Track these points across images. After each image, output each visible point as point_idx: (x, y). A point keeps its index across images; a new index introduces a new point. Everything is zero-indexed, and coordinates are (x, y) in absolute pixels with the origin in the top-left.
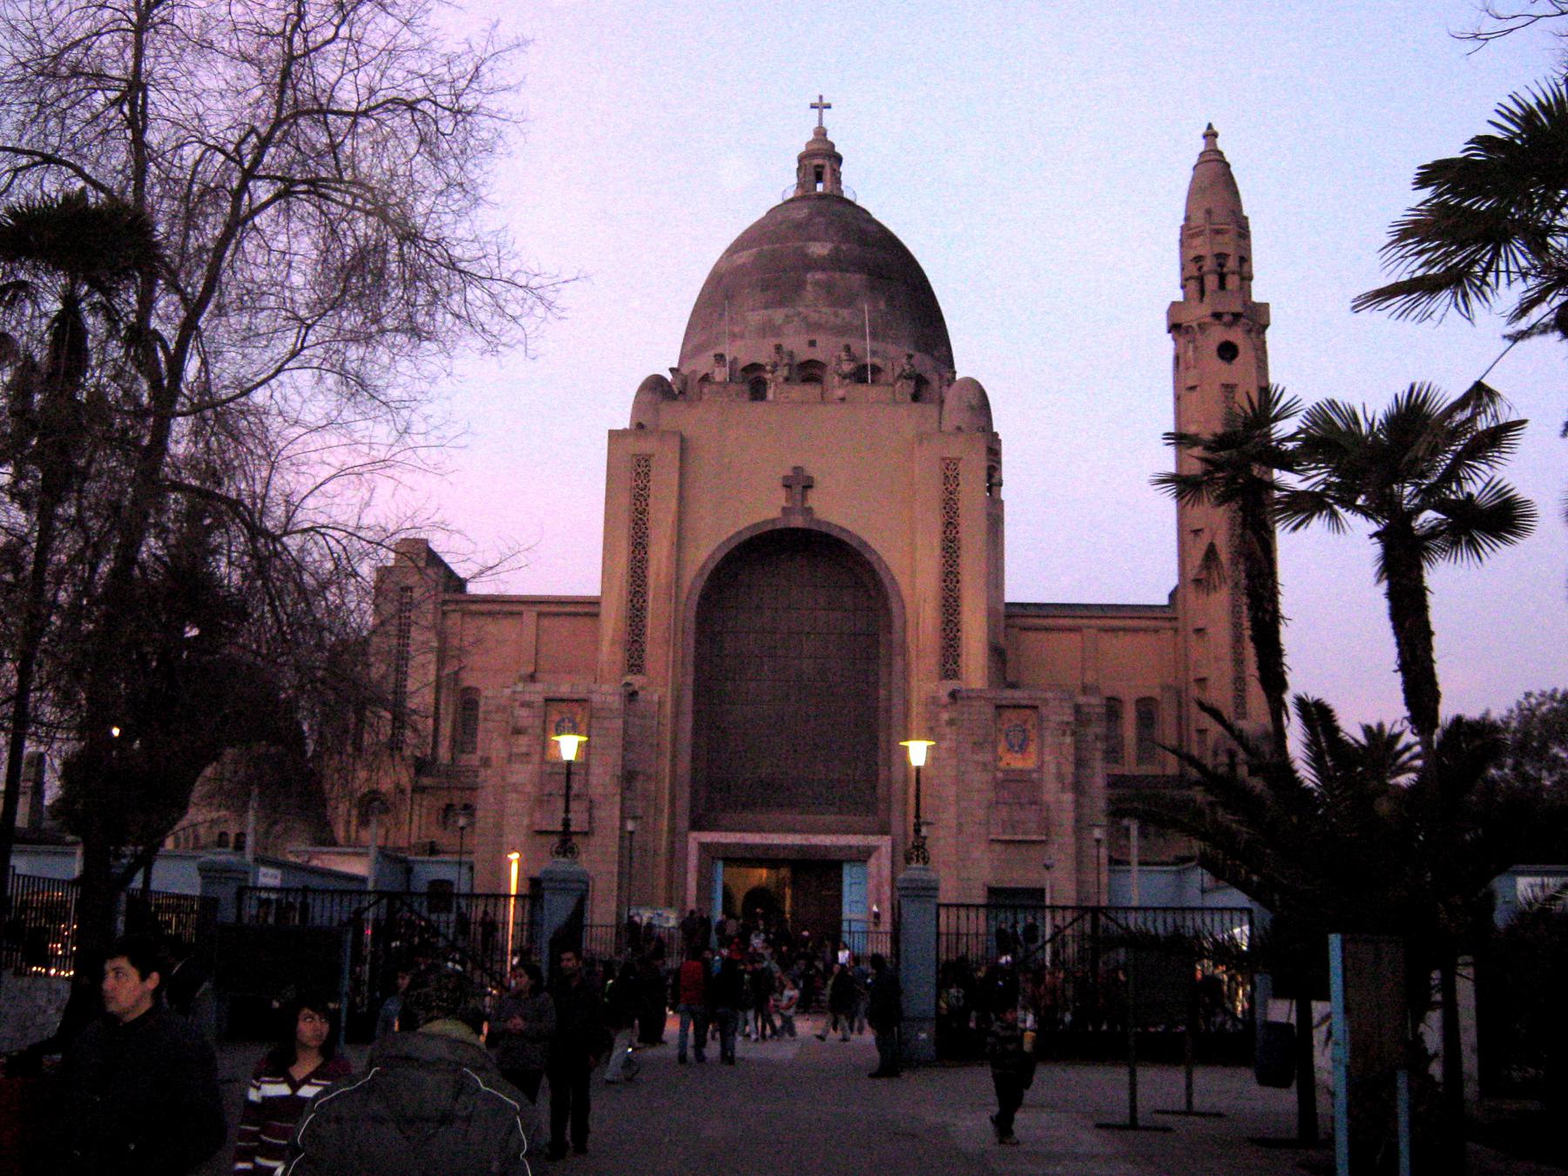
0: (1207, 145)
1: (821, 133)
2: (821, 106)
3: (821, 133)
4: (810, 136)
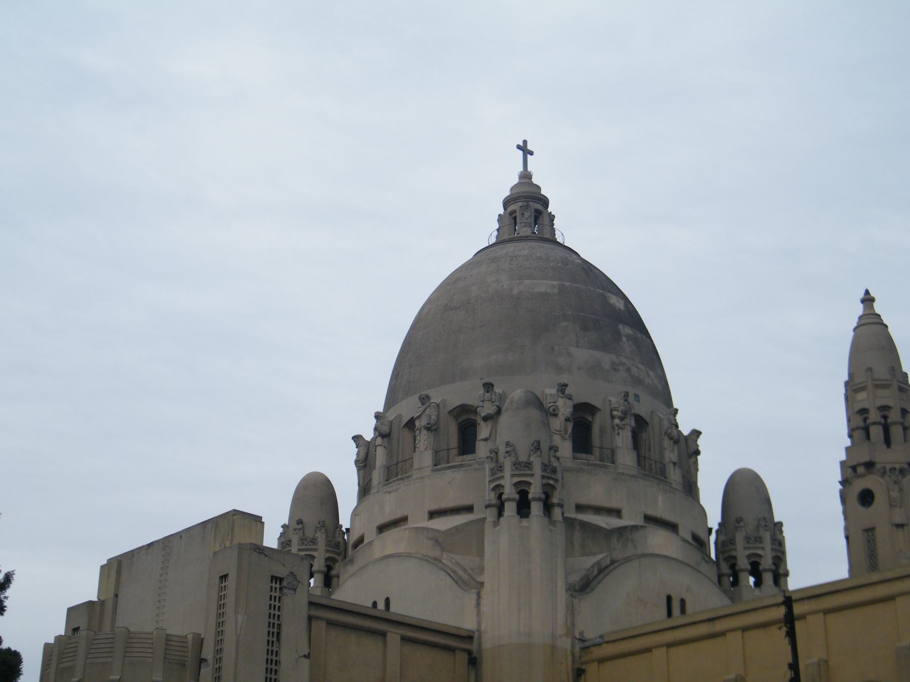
0: (865, 308)
1: (526, 176)
2: (524, 149)
3: (526, 176)
4: (516, 180)
